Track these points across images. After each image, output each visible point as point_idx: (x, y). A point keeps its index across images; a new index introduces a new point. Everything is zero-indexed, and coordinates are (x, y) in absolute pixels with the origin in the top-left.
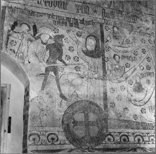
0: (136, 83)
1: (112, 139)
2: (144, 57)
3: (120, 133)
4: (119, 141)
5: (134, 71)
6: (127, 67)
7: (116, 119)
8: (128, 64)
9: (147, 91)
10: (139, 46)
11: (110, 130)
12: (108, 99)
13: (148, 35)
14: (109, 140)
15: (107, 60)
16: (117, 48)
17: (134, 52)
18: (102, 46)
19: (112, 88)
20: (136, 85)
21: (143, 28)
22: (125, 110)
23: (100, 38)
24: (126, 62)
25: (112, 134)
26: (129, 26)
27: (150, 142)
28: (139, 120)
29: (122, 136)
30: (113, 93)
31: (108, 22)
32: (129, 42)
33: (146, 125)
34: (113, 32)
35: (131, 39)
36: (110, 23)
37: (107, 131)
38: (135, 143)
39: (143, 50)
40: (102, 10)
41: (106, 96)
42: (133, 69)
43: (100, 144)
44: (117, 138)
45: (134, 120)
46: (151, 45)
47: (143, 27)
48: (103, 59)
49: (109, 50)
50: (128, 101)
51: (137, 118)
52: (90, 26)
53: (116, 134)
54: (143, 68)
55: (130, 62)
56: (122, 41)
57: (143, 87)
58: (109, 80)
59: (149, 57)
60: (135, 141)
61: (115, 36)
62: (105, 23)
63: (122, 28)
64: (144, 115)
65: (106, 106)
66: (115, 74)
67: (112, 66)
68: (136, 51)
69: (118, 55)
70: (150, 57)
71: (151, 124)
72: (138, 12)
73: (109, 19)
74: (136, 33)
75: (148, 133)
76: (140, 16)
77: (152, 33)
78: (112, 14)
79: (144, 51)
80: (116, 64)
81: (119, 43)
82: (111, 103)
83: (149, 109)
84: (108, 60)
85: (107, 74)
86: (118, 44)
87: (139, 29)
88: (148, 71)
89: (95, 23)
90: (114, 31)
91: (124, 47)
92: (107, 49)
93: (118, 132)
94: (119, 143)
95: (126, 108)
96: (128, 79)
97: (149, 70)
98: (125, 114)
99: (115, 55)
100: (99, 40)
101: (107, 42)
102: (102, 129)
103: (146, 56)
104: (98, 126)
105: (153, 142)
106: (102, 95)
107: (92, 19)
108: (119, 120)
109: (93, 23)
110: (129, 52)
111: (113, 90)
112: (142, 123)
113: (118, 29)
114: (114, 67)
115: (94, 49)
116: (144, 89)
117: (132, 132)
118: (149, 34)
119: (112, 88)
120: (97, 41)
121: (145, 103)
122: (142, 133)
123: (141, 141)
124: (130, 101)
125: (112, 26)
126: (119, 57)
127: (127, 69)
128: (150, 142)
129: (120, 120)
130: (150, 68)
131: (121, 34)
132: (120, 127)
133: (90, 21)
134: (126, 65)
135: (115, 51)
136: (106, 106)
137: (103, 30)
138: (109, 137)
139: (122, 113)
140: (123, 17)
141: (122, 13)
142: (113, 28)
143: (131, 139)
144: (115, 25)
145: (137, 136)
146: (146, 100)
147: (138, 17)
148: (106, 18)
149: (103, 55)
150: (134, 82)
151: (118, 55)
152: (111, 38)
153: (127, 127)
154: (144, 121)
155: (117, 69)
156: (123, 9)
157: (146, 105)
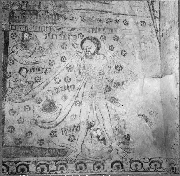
0: (47, 100)
2: (64, 66)
3: (16, 162)
4: (15, 171)
5: (46, 85)
6: (36, 82)
7: (14, 146)
8: (39, 78)
9: (61, 110)
10: (57, 53)
12: (5, 123)
13: (72, 38)
15: (9, 76)
16: (25, 59)
17: (50, 62)
19: (12, 110)
20: (47, 103)
22: (28, 134)
24: (36, 76)
25: (6, 163)
27: (57, 172)
28: (45, 146)
29: (20, 165)
30: (13, 115)
31: (16, 28)
32: (43, 50)
33: (56, 150)
34: (22, 39)
36: (19, 29)
38: (38, 173)
39: (63, 58)
40: (10, 13)
42: (45, 83)
45: (39, 146)
46: (75, 50)
49: (13, 64)
50: (33, 123)
51: (43, 143)
53: (11, 164)
54: (60, 81)
55: (42, 75)
56: (33, 49)
57: (56, 104)
58: (10, 100)
59: (70, 66)
60: (37, 170)
61: (24, 45)
62: (12, 29)
63: (35, 33)
64: (53, 139)
66: (18, 92)
67: (15, 82)
68: (52, 61)
69: (25, 68)
70: (72, 66)
71: (63, 149)
72: (62, 9)
73: (18, 24)
74: (55, 37)
75: (57, 161)
76: (64, 13)
77: (79, 34)
79: (64, 58)
80: (22, 80)
81: (29, 52)
82: (9, 128)
83: (62, 132)
84: (10, 76)
85: (8, 93)
86: (28, 54)
87: (61, 31)
88: (66, 84)
90: (23, 38)
91: (35, 57)
92: (11, 62)
93: (14, 162)
94: (15, 173)
95: (30, 132)
96: (36, 96)
97: (69, 82)
98: (27, 140)
99: (21, 69)
101: (12, 53)
103: (66, 65)
105: (62, 171)
108: (17, 147)
110: (42, 62)
111: (13, 112)
112: (49, 149)
113: (29, 34)
114: (18, 83)
116: (57, 108)
117: (34, 160)
118: (74, 36)
119: (12, 110)
121: (57, 125)
122: (48, 161)
123: (46, 170)
124: (36, 122)
126: (27, 71)
127: (36, 84)
128: (57, 172)
129: (19, 147)
130: (70, 79)
131: (32, 42)
132: (19, 155)
134: (35, 79)
135: (22, 63)
137: (8, 39)
139: (22, 138)
140: (39, 18)
141: (37, 14)
142: (23, 34)
144: (26, 30)
145: (40, 164)
146: (58, 121)
147: (61, 16)
148: (15, 24)
150: (44, 100)
151: (26, 67)
152: (18, 48)
153: (27, 155)
154: (55, 146)
155: (22, 86)
157: (58, 127)
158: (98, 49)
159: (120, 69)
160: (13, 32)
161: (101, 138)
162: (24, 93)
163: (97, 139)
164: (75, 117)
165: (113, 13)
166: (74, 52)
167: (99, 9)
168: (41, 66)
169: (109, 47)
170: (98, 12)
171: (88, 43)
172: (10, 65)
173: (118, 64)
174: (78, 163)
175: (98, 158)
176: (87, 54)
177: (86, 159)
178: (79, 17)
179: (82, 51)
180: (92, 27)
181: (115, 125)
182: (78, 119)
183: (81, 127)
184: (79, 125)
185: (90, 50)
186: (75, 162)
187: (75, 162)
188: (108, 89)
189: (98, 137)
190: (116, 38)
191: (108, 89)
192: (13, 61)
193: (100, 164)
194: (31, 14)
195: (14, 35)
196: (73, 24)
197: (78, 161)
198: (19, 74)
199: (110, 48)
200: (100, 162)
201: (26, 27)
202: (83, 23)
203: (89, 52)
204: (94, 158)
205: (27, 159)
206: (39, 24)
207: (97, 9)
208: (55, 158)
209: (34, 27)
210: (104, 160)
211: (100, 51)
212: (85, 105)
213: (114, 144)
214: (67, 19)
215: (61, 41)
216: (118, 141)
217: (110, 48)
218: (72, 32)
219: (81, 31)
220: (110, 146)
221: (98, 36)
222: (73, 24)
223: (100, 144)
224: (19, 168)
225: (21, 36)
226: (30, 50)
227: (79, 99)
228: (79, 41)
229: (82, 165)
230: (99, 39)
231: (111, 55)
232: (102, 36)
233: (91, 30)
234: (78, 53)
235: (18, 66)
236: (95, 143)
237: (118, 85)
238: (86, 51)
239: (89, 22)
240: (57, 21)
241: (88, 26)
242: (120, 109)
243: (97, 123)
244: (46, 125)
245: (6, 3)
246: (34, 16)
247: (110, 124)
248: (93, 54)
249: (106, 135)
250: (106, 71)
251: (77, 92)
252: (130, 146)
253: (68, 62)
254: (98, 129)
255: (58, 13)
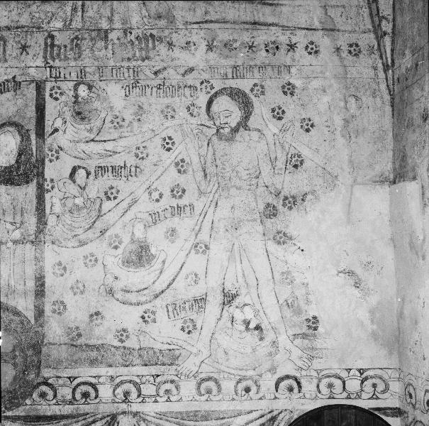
0: (133, 241)
1: (50, 393)
2: (169, 161)
3: (71, 379)
4: (70, 397)
5: (130, 207)
6: (109, 198)
7: (65, 344)
8: (114, 191)
9: (164, 262)
10: (153, 131)
11: (46, 373)
13: (187, 91)
14: (43, 395)
15: (49, 188)
16: (83, 146)
17: (138, 151)
18: (40, 149)
19: (60, 264)
20: (134, 247)
21: (171, 71)
22: (95, 317)
23: (31, 126)
24: (109, 183)
25: (50, 381)
26: (126, 75)
27: (158, 398)
28: (132, 343)
29: (79, 385)
30: (62, 275)
32: (121, 123)
33: (154, 353)
34: (73, 99)
35: (128, 116)
36: (67, 76)
37: (38, 375)
38: (117, 400)
39: (167, 140)
40: (46, 39)
41: (43, 285)
42: (128, 201)
43: (18, 406)
44: (66, 392)
45: (119, 344)
46: (194, 121)
47: (175, 68)
48: (40, 187)
49: (57, 158)
50: (104, 294)
51: (127, 337)
52: (8, 95)
53: (61, 382)
54: (161, 196)
55: (120, 184)
56: (98, 123)
57: (153, 251)
59: (183, 161)
60: (115, 396)
61: (79, 113)
62: (51, 77)
63: (102, 84)
64: (150, 328)
65: (40, 313)
66: (69, 223)
68: (142, 148)
69: (84, 168)
70: (187, 160)
71: (170, 350)
72: (163, 23)
74: (148, 91)
75: (158, 376)
76: (167, 32)
77: (202, 83)
78: (77, 45)
80: (77, 195)
81: (90, 131)
83: (168, 311)
84: (53, 188)
85: (48, 227)
86: (88, 134)
87: (161, 76)
88: (174, 202)
89: (22, 83)
90: (76, 97)
91: (105, 141)
93: (67, 378)
94: (70, 402)
95: (97, 314)
96: (108, 234)
97: (181, 197)
98: (91, 330)
99: (74, 170)
100: (30, 133)
101: (53, 133)
102: (25, 371)
104: (15, 365)
105: (169, 398)
106: (31, 284)
107: (15, 72)
108: (72, 345)
109: (18, 85)
110: (119, 153)
111: (63, 268)
112: (140, 349)
113: (90, 88)
114: (69, 203)
115: (13, 162)
116: (155, 257)
117: (109, 374)
118: (190, 87)
119: (60, 264)
120: (25, 136)
121: (156, 296)
122: (138, 376)
123: (134, 395)
124: (111, 292)
125: (71, 84)
126: (88, 174)
127: (107, 205)
128: (158, 398)
130: (184, 191)
131: (97, 104)
132: (77, 363)
133: (7, 81)
134: (106, 193)
135: (75, 157)
136: (40, 313)
137: (44, 99)
138: (44, 388)
139: (82, 326)
140: (110, 47)
141: (106, 37)
143: (105, 392)
144: (81, 78)
145: (122, 383)
146: (159, 287)
147: (160, 40)
148: (57, 63)
149: (41, 174)
150: (126, 239)
152: (66, 122)
153: (93, 362)
154: (151, 344)
155: (79, 208)
156: (110, 20)
157: (158, 302)
158: (247, 117)
159: (296, 163)
160: (54, 84)
161: (252, 326)
162: (83, 224)
163: (243, 328)
164: (194, 279)
165: (283, 26)
166: (193, 126)
167: (248, 19)
168: (117, 161)
169: (273, 111)
170: (247, 26)
171: (223, 103)
172: (51, 161)
173: (293, 151)
174: (204, 380)
175: (246, 370)
176: (221, 130)
177: (220, 372)
178: (202, 40)
179: (210, 123)
180: (233, 63)
181: (285, 297)
182: (201, 282)
183: (209, 301)
184: (204, 297)
185: (228, 120)
186: (195, 377)
187: (195, 377)
188: (271, 212)
189: (247, 323)
190: (289, 89)
191: (271, 212)
192: (57, 152)
193: (249, 383)
194: (92, 39)
195: (56, 90)
196: (186, 59)
197: (203, 376)
198: (70, 181)
199: (276, 113)
200: (251, 378)
201: (82, 72)
202: (211, 55)
203: (227, 125)
204: (237, 369)
205: (95, 371)
206: (112, 63)
207: (244, 18)
208: (153, 370)
209: (99, 69)
210: (259, 373)
211: (252, 122)
212: (218, 251)
213: (283, 340)
214: (174, 46)
215: (161, 100)
216: (291, 332)
217: (276, 113)
218: (187, 77)
219: (206, 76)
220: (274, 342)
221: (245, 85)
222: (186, 59)
223: (252, 338)
224: (79, 391)
225: (72, 93)
226: (92, 125)
227: (204, 236)
228: (202, 99)
229: (211, 384)
230: (248, 91)
231: (276, 131)
232: (255, 85)
233: (230, 71)
234: (201, 127)
235: (67, 163)
236: (239, 336)
237: (292, 202)
238: (218, 123)
239: (226, 51)
240: (151, 54)
241: (223, 62)
242: (295, 258)
243: (243, 291)
244: (133, 298)
245: (37, 15)
246: (101, 44)
247: (274, 293)
248: (235, 130)
249: (264, 318)
250: (266, 169)
251: (199, 222)
252: (318, 343)
253: (179, 151)
254: (245, 305)
255: (154, 32)
